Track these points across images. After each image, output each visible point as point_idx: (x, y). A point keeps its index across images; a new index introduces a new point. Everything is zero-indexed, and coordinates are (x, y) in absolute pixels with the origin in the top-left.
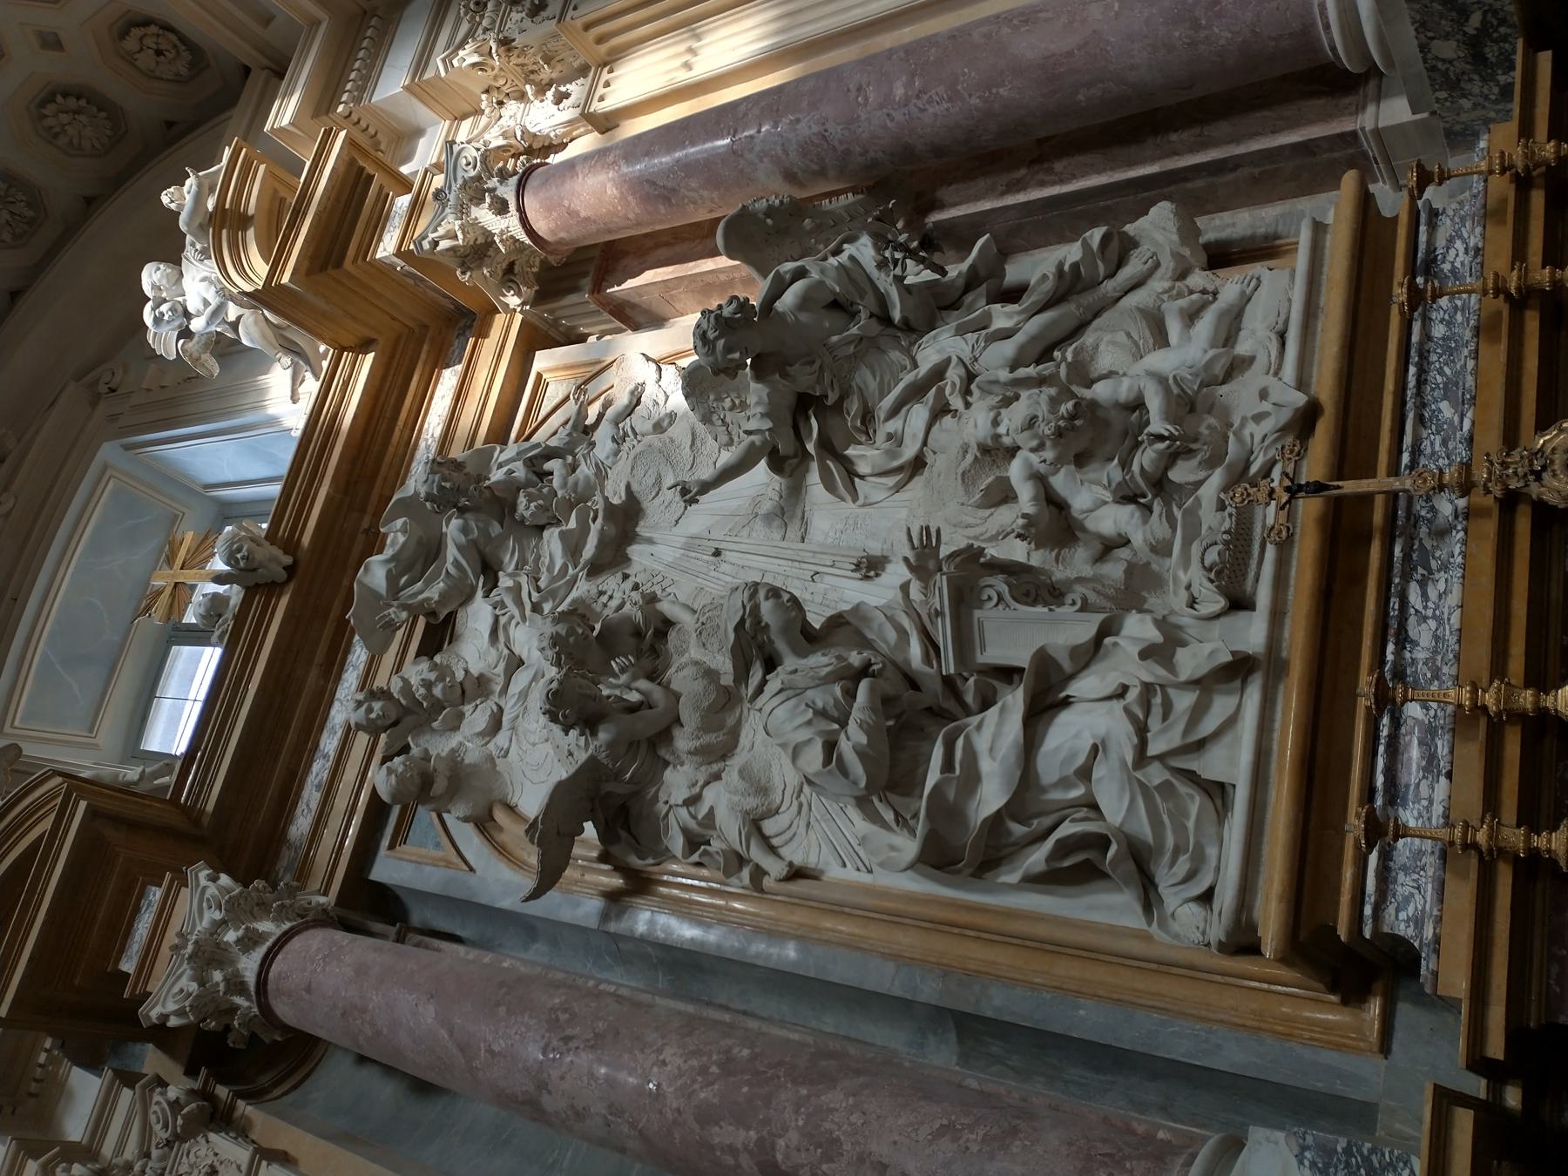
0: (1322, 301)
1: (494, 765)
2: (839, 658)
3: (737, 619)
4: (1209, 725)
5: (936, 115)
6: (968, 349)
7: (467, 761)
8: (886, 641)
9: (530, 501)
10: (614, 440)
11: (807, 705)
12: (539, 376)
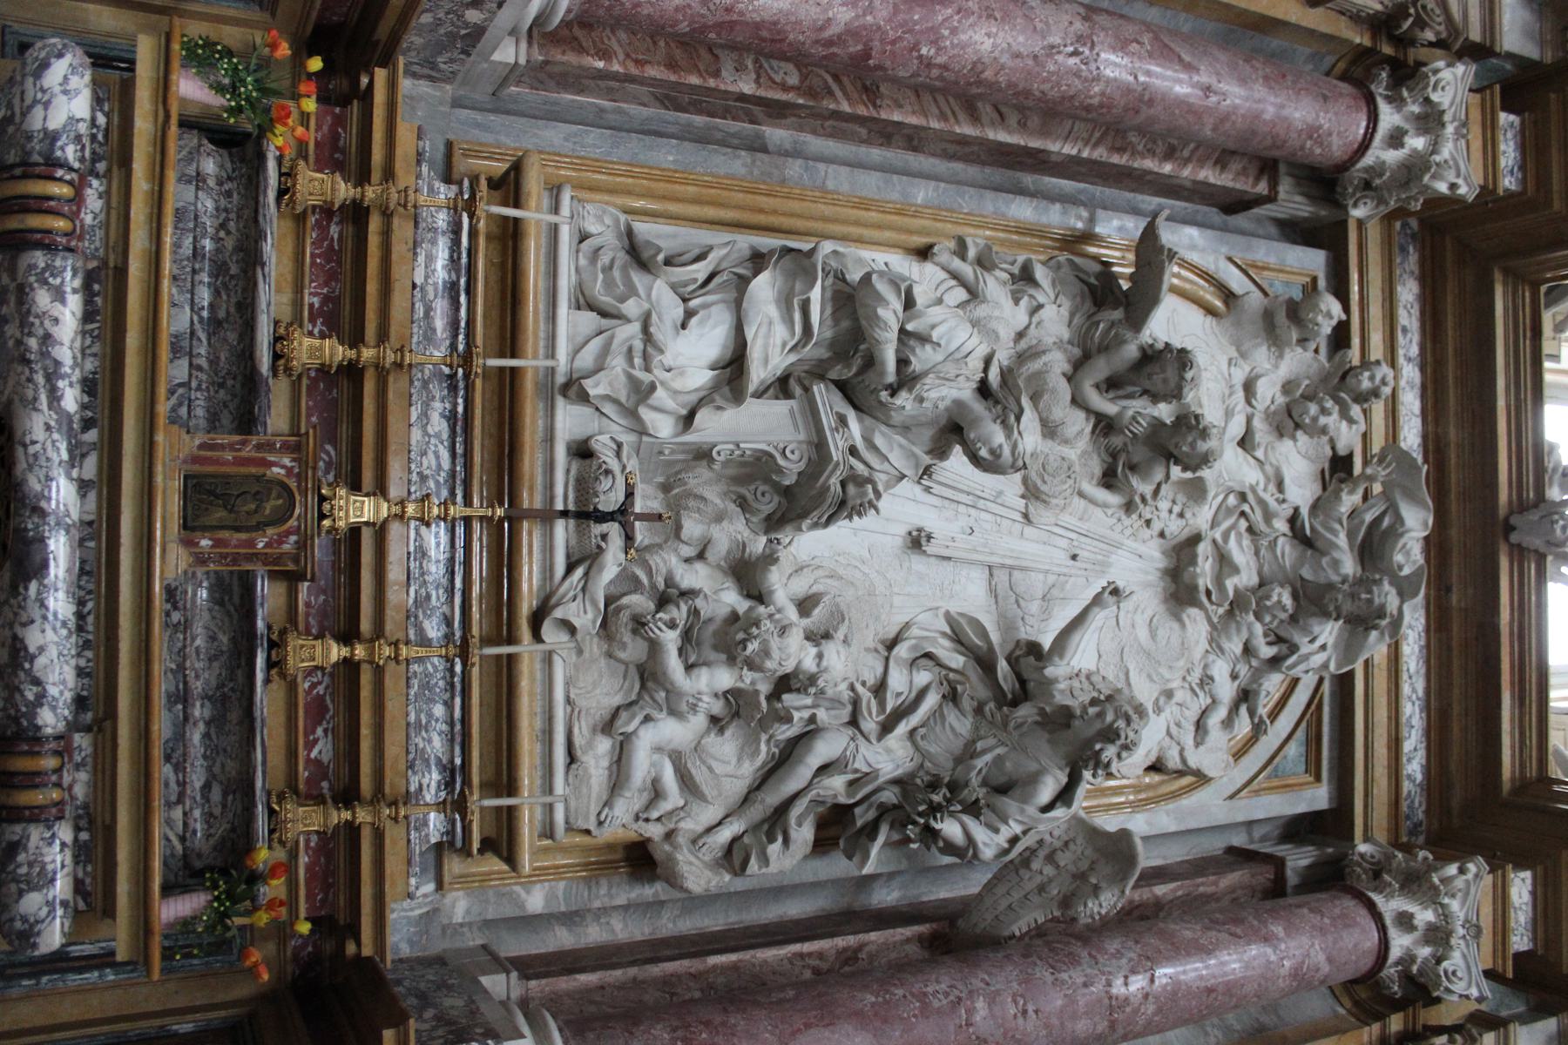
0: (538, 747)
1: (1238, 350)
2: (921, 400)
3: (1024, 419)
4: (595, 345)
5: (938, 982)
6: (862, 749)
7: (1264, 348)
8: (883, 434)
9: (1279, 602)
10: (1212, 679)
11: (939, 345)
12: (1318, 778)
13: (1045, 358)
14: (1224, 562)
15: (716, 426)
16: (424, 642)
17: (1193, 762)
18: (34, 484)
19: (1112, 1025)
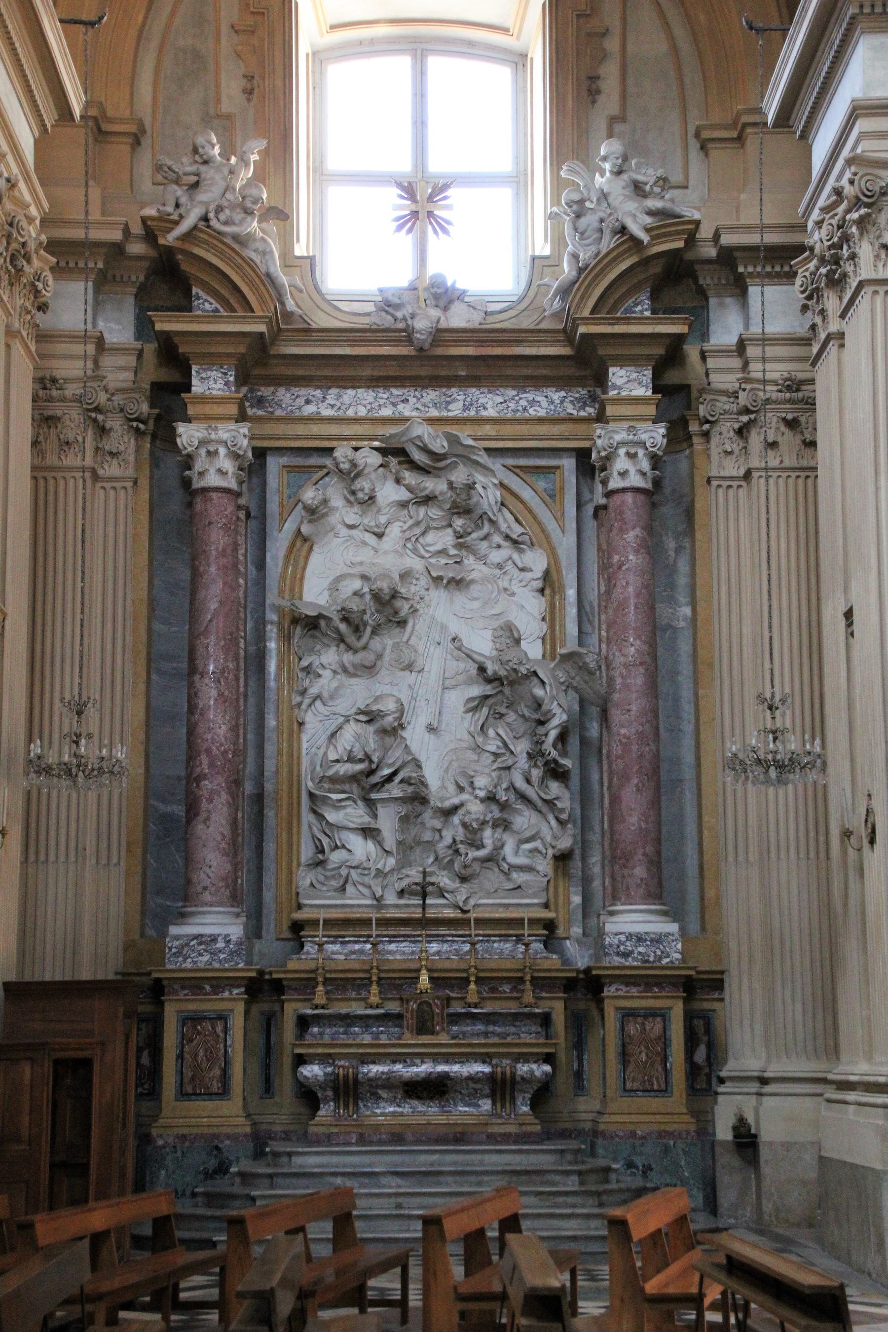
4: (361, 888)
12: (558, 467)
13: (347, 664)
14: (443, 552)
15: (390, 842)
16: (470, 951)
17: (539, 574)
18: (423, 1075)
19: (641, 664)
